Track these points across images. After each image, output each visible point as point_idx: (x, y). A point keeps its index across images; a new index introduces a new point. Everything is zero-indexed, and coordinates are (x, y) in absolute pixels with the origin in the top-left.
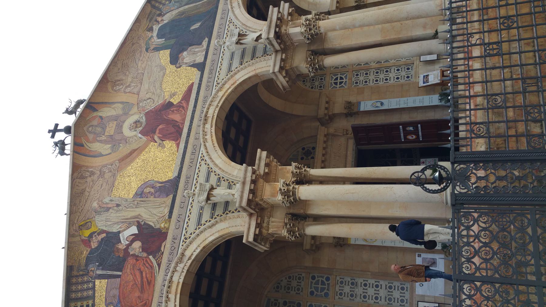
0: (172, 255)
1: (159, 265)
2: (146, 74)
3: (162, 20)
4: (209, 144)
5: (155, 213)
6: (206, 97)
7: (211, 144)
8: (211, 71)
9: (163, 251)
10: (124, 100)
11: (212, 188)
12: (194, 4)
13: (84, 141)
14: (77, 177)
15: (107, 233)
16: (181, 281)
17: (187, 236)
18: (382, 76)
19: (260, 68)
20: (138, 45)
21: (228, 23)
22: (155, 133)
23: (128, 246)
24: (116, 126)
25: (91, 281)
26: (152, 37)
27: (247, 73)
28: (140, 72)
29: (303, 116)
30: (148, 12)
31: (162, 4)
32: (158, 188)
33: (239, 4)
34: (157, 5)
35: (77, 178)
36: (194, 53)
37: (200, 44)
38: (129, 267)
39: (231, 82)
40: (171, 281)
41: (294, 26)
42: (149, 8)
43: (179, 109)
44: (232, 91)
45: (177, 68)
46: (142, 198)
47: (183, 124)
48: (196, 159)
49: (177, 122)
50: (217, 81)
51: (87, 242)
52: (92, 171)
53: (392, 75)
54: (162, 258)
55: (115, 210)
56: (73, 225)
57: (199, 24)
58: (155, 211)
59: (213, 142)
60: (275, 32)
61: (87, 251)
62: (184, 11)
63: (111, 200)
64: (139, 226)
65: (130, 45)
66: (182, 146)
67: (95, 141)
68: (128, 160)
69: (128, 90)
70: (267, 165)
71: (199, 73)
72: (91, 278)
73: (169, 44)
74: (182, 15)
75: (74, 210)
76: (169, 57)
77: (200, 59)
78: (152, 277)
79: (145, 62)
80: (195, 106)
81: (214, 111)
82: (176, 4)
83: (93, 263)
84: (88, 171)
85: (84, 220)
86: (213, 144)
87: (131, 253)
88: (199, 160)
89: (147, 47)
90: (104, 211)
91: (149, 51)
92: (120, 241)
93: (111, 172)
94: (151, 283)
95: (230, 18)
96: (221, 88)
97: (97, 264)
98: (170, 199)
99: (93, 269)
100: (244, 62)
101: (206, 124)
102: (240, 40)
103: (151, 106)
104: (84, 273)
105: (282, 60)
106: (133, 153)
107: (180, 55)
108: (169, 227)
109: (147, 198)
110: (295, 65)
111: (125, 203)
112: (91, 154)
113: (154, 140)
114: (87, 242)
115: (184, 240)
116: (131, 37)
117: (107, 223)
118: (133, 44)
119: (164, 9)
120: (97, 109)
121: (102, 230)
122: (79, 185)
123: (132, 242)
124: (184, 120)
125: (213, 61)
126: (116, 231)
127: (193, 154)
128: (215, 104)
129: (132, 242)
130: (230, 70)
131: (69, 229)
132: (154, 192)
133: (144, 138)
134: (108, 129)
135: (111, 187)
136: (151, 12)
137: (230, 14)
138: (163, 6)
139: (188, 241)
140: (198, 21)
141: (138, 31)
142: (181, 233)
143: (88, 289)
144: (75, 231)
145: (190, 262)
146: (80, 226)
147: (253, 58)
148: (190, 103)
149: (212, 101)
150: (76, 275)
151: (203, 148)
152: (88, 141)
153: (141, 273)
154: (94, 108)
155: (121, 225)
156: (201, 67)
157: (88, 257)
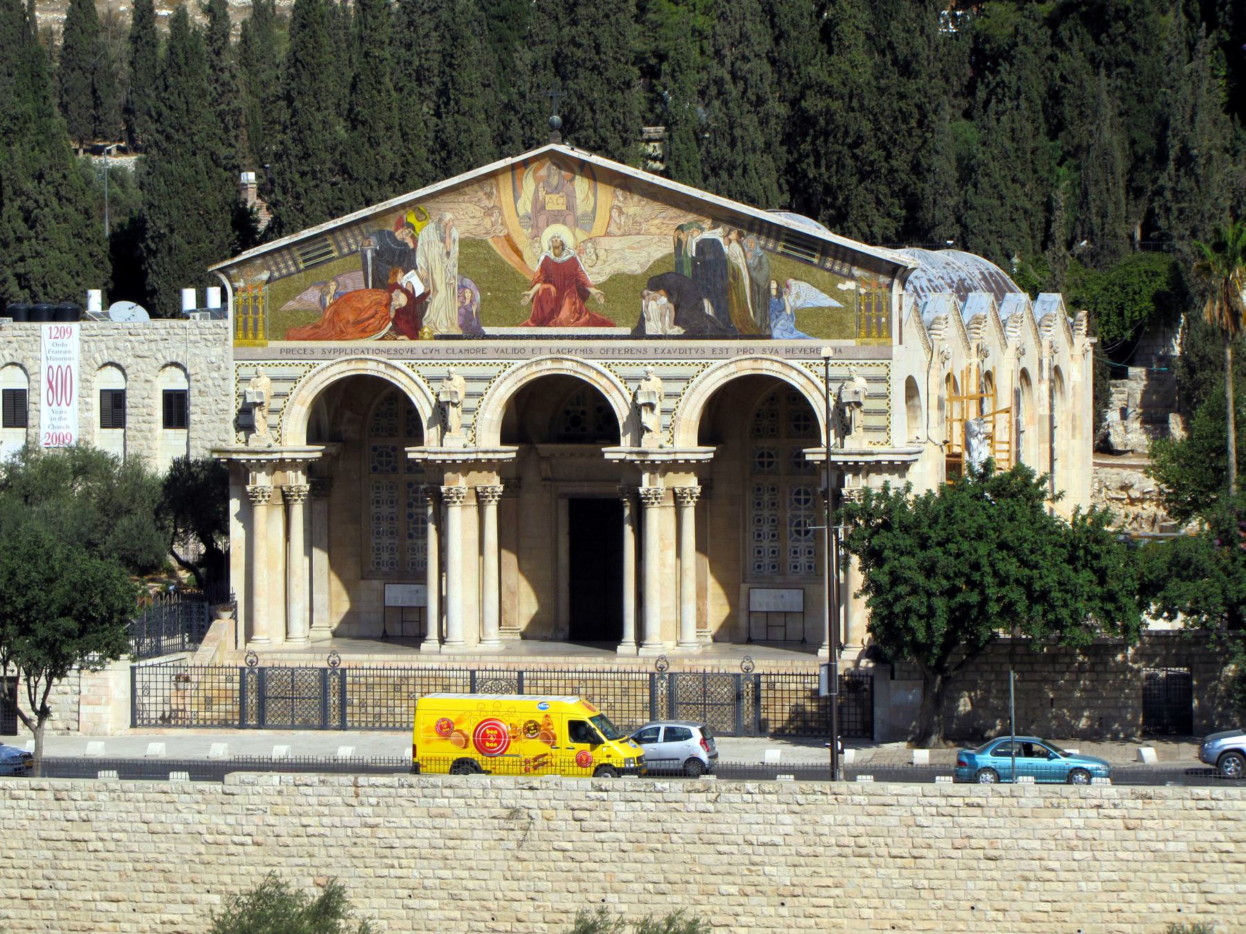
1: (382, 339)
4: (524, 372)
6: (591, 350)
11: (455, 405)
15: (414, 250)
16: (369, 373)
17: (416, 368)
18: (766, 528)
21: (704, 361)
22: (545, 282)
26: (702, 230)
36: (662, 316)
37: (677, 322)
47: (556, 325)
51: (401, 224)
53: (766, 544)
58: (442, 315)
67: (537, 180)
68: (509, 250)
69: (615, 214)
70: (489, 460)
71: (627, 331)
77: (651, 328)
80: (579, 338)
92: (406, 272)
94: (364, 333)
107: (662, 292)
112: (517, 183)
114: (401, 224)
123: (406, 291)
124: (561, 325)
125: (645, 350)
129: (406, 291)
133: (536, 267)
134: (554, 197)
139: (409, 371)
140: (716, 308)
145: (388, 378)
149: (582, 363)
152: (535, 171)
153: (373, 317)
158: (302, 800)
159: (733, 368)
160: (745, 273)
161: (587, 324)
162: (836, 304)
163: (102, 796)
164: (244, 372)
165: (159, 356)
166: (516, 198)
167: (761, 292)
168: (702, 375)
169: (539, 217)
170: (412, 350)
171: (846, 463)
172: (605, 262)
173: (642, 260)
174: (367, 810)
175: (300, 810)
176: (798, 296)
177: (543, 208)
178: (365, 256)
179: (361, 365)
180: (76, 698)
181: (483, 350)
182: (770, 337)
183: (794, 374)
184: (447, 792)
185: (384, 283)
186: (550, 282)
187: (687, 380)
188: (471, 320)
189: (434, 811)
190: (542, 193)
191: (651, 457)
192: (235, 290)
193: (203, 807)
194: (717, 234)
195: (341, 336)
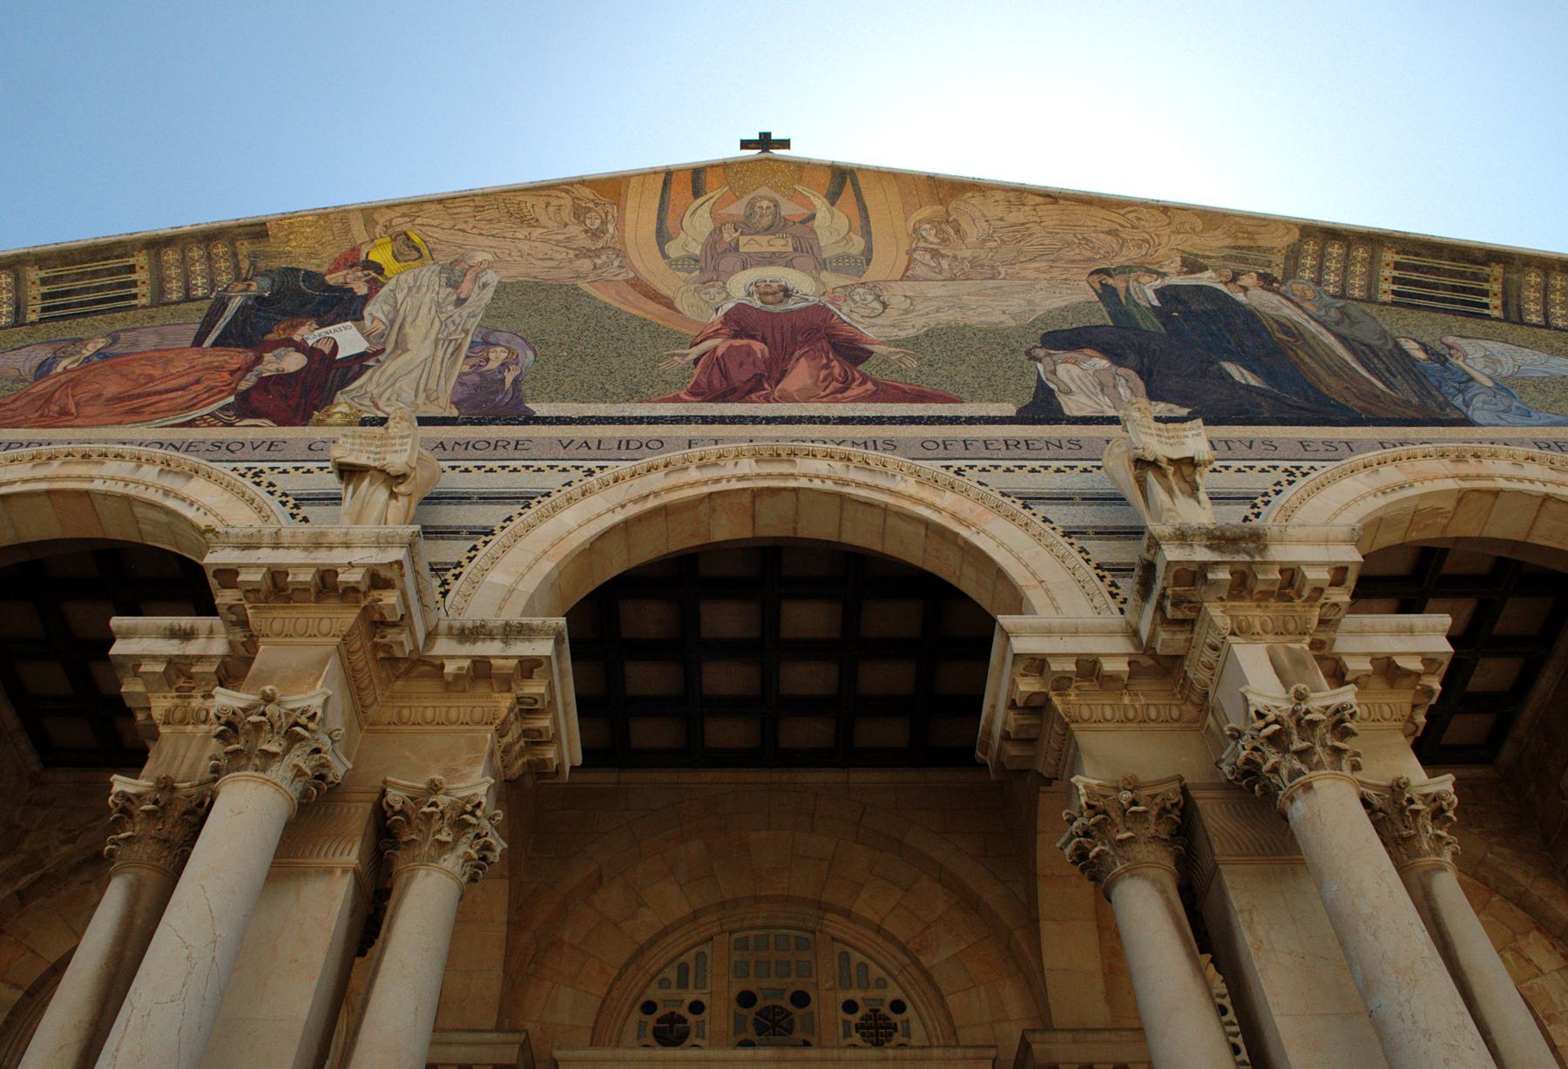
0: (211, 448)
2: (991, 283)
3: (1245, 289)
4: (657, 480)
5: (397, 385)
6: (891, 445)
7: (656, 487)
8: (1022, 445)
9: (237, 424)
12: (1349, 358)
13: (718, 196)
14: (578, 199)
15: (365, 299)
17: (265, 479)
19: (1053, 599)
20: (1114, 246)
22: (735, 337)
23: (301, 347)
24: (774, 253)
25: (212, 290)
26: (1164, 275)
27: (1019, 559)
28: (1002, 270)
29: (1042, 972)
30: (1261, 243)
31: (1320, 275)
32: (500, 377)
33: (1402, 487)
34: (1309, 262)
35: (573, 198)
37: (1153, 395)
38: (221, 358)
39: (966, 507)
41: (1285, 661)
42: (1282, 241)
43: (837, 381)
44: (926, 524)
45: (1028, 353)
46: (470, 348)
47: (767, 400)
48: (600, 454)
49: (777, 384)
50: (971, 467)
51: (352, 260)
52: (604, 232)
54: (210, 426)
55: (445, 299)
56: (404, 215)
57: (1253, 381)
58: (406, 386)
59: (669, 490)
60: (1205, 566)
61: (319, 266)
62: (1307, 335)
63: (485, 286)
64: (362, 356)
65: (1107, 226)
68: (633, 295)
70: (481, 670)
72: (225, 290)
73: (1138, 317)
74: (1286, 333)
75: (458, 210)
76: (1074, 326)
78: (153, 413)
79: (1045, 276)
81: (817, 477)
82: (1333, 313)
83: (273, 285)
84: (604, 223)
85: (425, 242)
86: (656, 494)
87: (268, 356)
88: (593, 465)
89: (1115, 270)
90: (449, 279)
91: (1095, 276)
92: (321, 325)
93: (595, 268)
95: (1312, 468)
97: (267, 295)
98: (441, 411)
99: (254, 287)
100: (1078, 544)
101: (757, 461)
102: (1154, 465)
104: (244, 271)
106: (660, 303)
107: (1088, 351)
108: (331, 425)
109: (467, 357)
110: (1084, 738)
111: (465, 314)
112: (670, 222)
113: (701, 342)
115: (253, 471)
116: (1139, 219)
117: (406, 291)
118: (1109, 232)
120: (839, 202)
121: (383, 285)
122: (551, 209)
124: (786, 398)
126: (366, 313)
127: (624, 443)
129: (311, 352)
130: (1027, 501)
131: (391, 206)
132: (486, 368)
133: (716, 318)
134: (763, 239)
135: (535, 277)
136: (1271, 250)
138: (1312, 280)
141: (1173, 232)
142: (288, 458)
143: (187, 289)
144: (386, 226)
146: (405, 233)
147: (1109, 570)
148: (862, 406)
150: (239, 252)
154: (839, 194)
155: (383, 319)
157: (298, 270)
159: (1390, 474)
160: (1313, 327)
161: (872, 398)
172: (906, 312)
173: (1016, 310)
177: (737, 249)
178: (221, 305)
182: (1467, 422)
186: (754, 337)
187: (1249, 499)
188: (497, 392)
191: (1280, 553)
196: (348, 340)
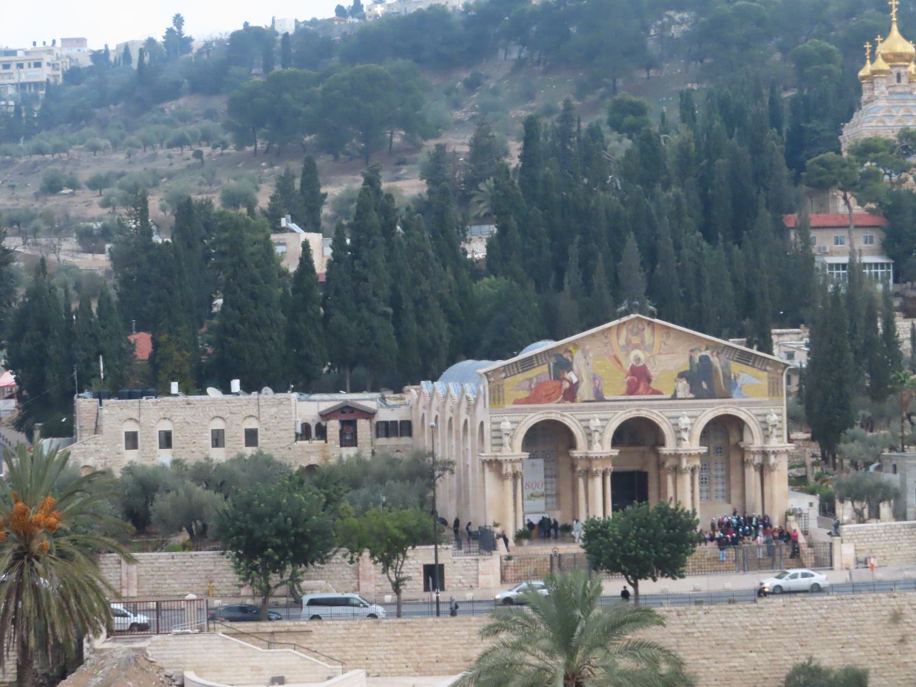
1: (558, 403)
2: (673, 355)
6: (653, 405)
10: (655, 344)
15: (572, 362)
22: (633, 375)
26: (701, 351)
36: (684, 389)
37: (691, 392)
39: (662, 421)
40: (551, 413)
64: (577, 383)
66: (623, 398)
67: (628, 330)
69: (662, 345)
71: (669, 396)
77: (680, 395)
92: (569, 372)
96: (658, 415)
103: (649, 368)
105: (670, 454)
107: (684, 379)
119: (722, 356)
128: (649, 414)
129: (568, 381)
133: (628, 369)
134: (635, 337)
137: (709, 409)
139: (571, 417)
140: (709, 386)
145: (561, 420)
151: (622, 412)
153: (554, 393)
156: (674, 397)
158: (793, 609)
162: (759, 382)
163: (700, 613)
164: (494, 420)
165: (243, 412)
166: (618, 337)
167: (727, 377)
168: (702, 415)
169: (629, 347)
170: (572, 408)
171: (774, 451)
174: (823, 611)
175: (793, 613)
176: (743, 379)
177: (630, 342)
179: (549, 415)
180: (475, 572)
181: (604, 407)
182: (731, 397)
183: (742, 413)
184: (858, 601)
185: (558, 377)
189: (852, 610)
190: (630, 336)
192: (489, 382)
193: (748, 614)
194: (708, 353)
195: (539, 402)
196: (572, 376)
